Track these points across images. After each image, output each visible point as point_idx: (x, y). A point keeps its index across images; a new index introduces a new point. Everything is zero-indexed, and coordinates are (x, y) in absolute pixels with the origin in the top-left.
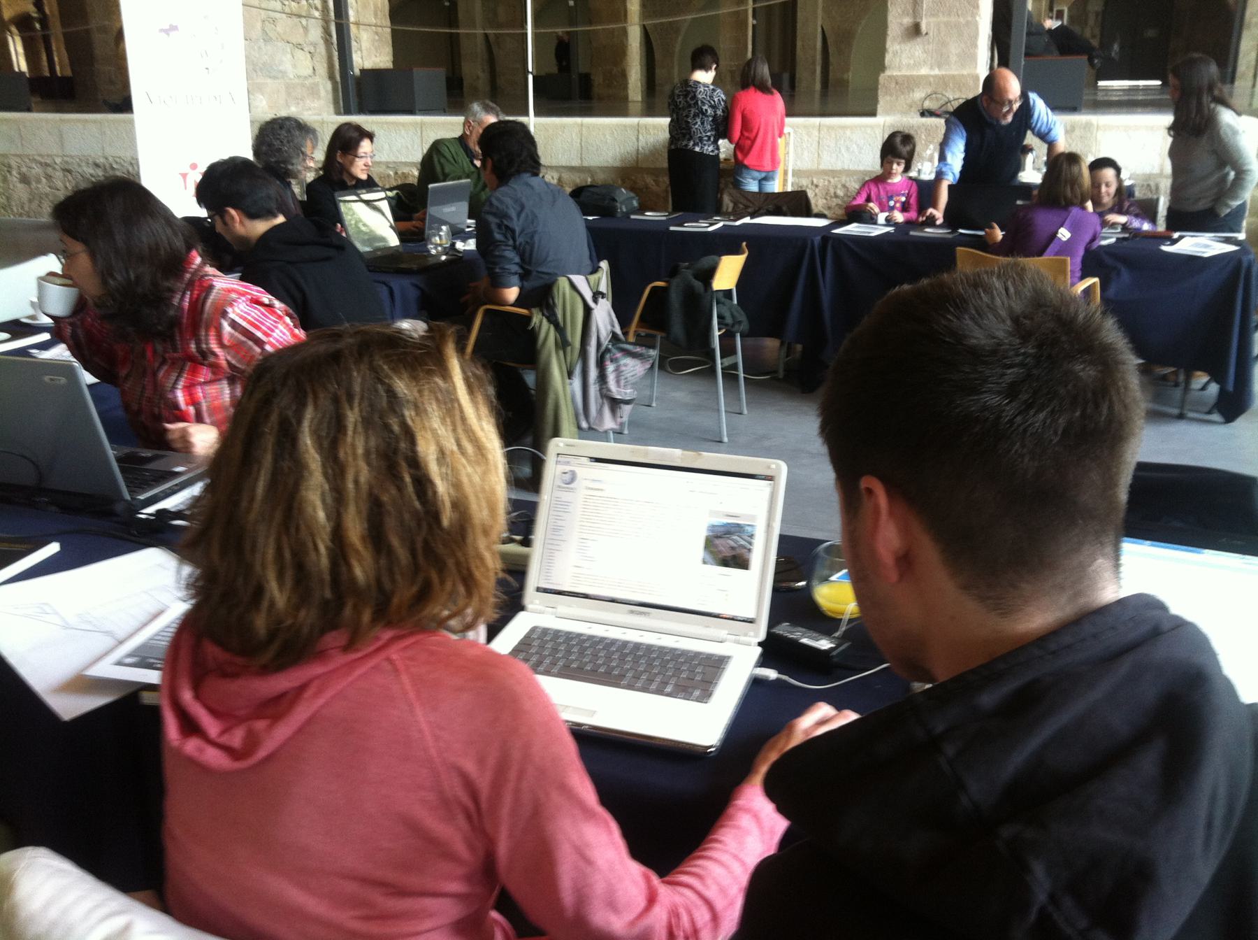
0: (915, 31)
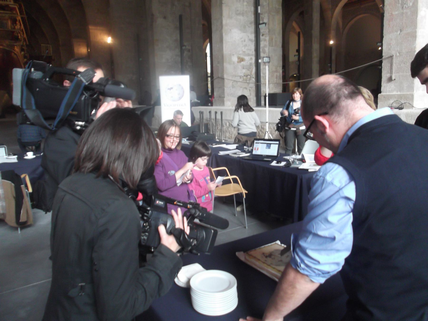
0: (390, 79)
